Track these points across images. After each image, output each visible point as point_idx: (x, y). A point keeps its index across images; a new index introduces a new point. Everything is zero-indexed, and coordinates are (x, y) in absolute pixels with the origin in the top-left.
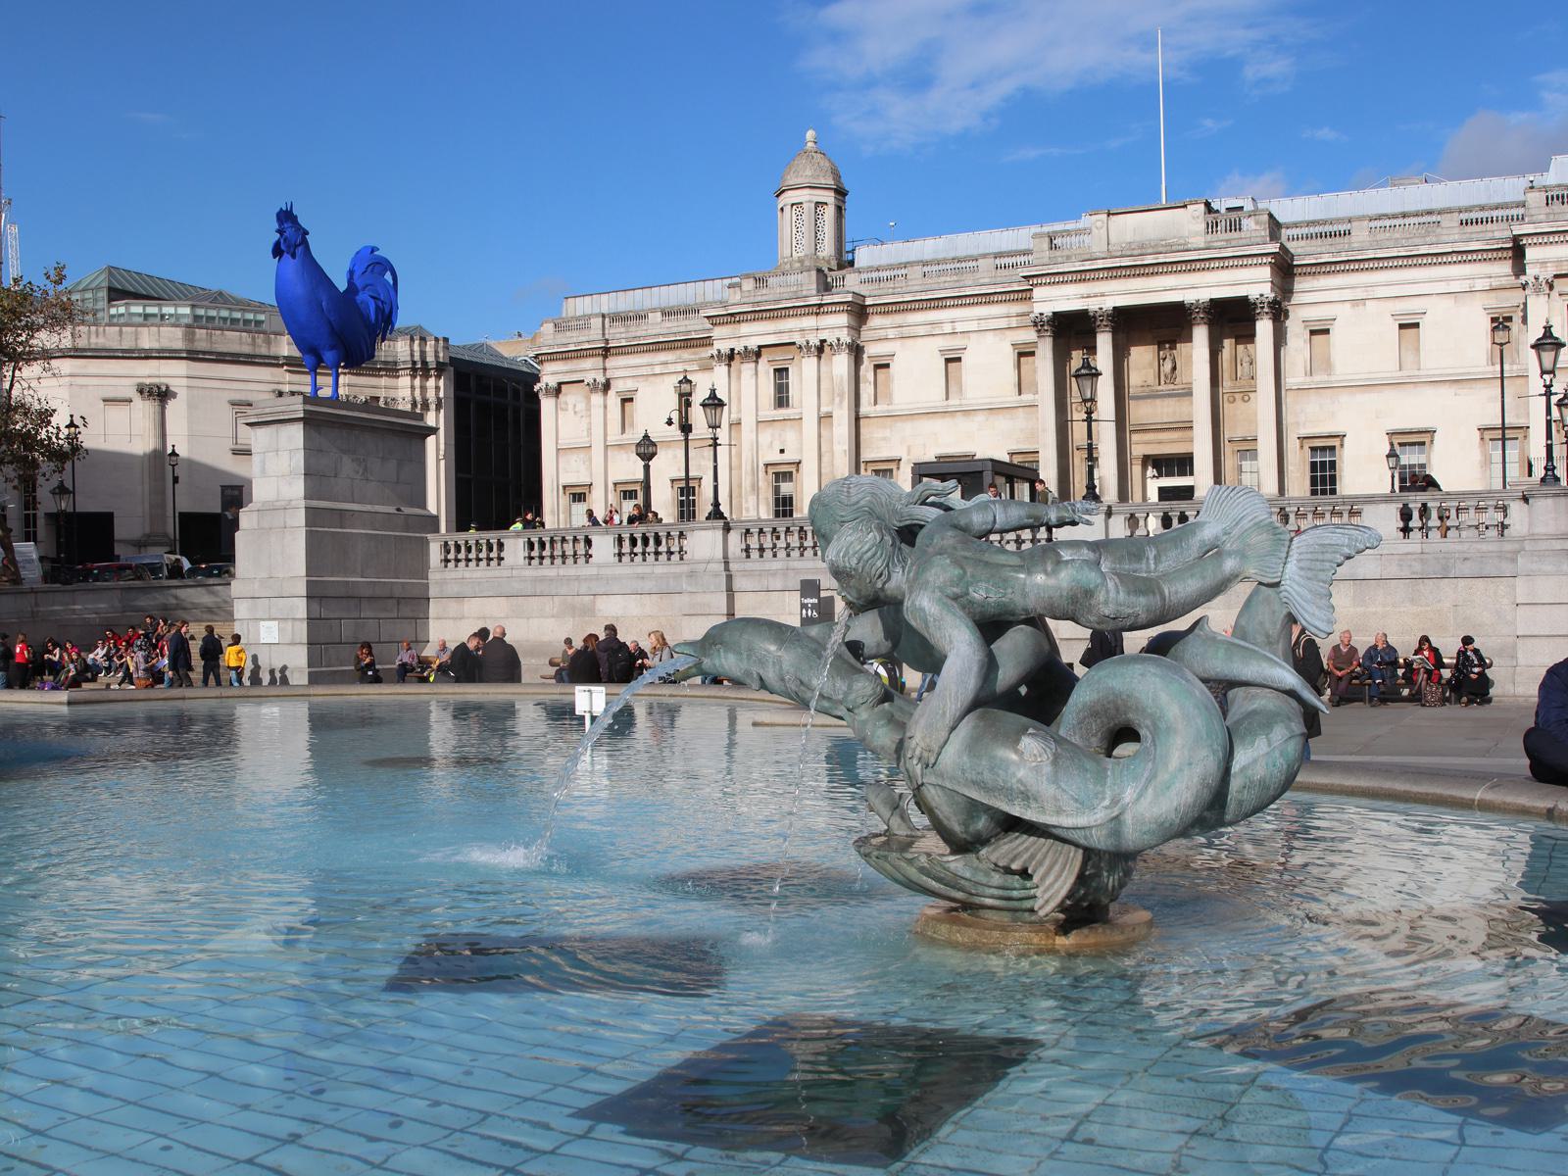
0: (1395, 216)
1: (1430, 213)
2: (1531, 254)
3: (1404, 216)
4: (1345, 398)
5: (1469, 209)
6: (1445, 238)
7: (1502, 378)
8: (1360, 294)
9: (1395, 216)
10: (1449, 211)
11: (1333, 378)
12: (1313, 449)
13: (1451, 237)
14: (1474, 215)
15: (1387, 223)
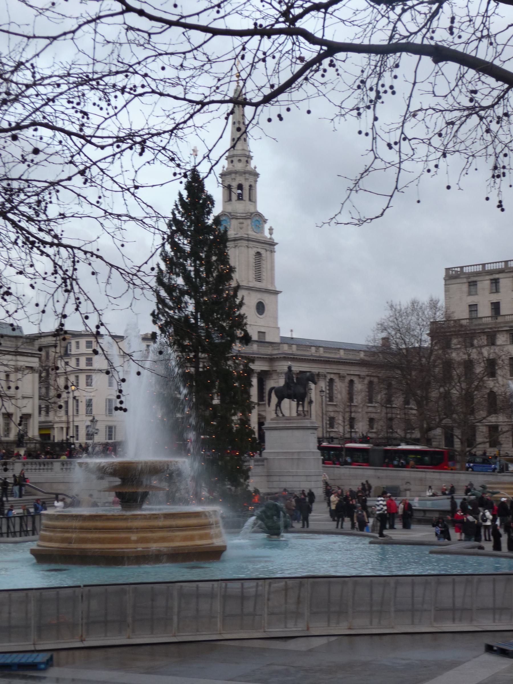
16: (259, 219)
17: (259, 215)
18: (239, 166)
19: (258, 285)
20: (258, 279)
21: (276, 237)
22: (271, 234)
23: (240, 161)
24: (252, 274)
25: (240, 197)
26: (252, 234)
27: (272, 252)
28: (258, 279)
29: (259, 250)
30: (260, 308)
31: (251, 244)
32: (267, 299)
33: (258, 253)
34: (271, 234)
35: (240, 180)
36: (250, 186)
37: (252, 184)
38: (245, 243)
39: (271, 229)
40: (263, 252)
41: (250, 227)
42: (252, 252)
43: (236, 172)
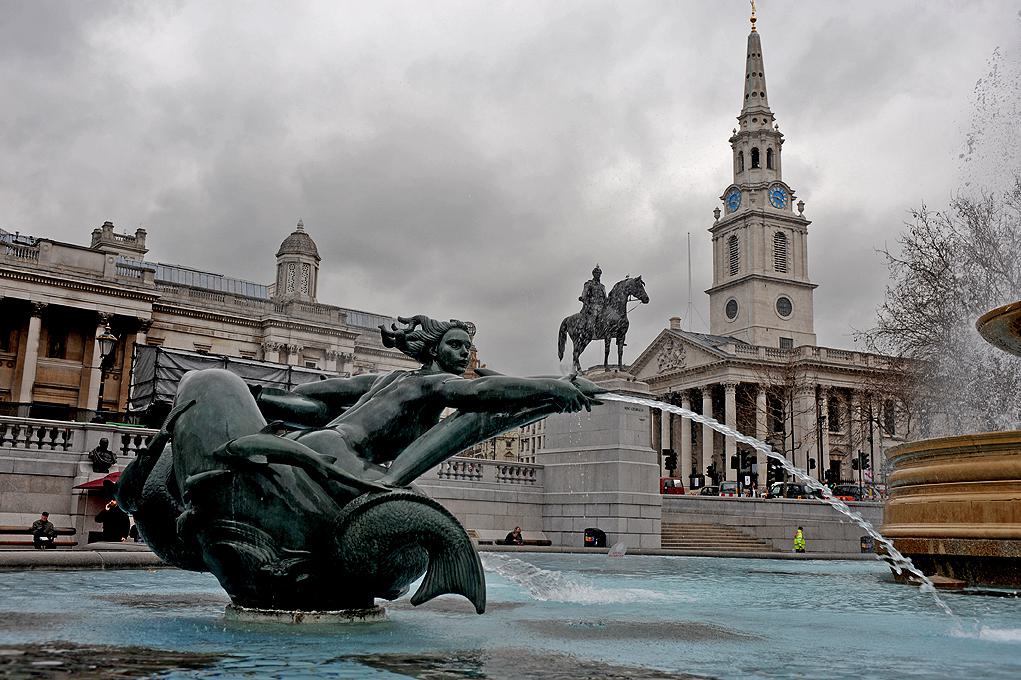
16: (784, 193)
17: (783, 186)
18: (753, 127)
19: (781, 275)
20: (782, 266)
21: (807, 215)
22: (801, 210)
23: (755, 120)
24: (770, 261)
25: (755, 165)
26: (769, 209)
27: (803, 233)
28: (782, 266)
29: (782, 230)
30: (784, 306)
31: (767, 221)
32: (794, 295)
33: (781, 235)
34: (801, 210)
35: (754, 143)
36: (770, 151)
37: (773, 147)
38: (757, 220)
39: (801, 204)
40: (787, 233)
41: (767, 199)
42: (771, 232)
43: (749, 134)
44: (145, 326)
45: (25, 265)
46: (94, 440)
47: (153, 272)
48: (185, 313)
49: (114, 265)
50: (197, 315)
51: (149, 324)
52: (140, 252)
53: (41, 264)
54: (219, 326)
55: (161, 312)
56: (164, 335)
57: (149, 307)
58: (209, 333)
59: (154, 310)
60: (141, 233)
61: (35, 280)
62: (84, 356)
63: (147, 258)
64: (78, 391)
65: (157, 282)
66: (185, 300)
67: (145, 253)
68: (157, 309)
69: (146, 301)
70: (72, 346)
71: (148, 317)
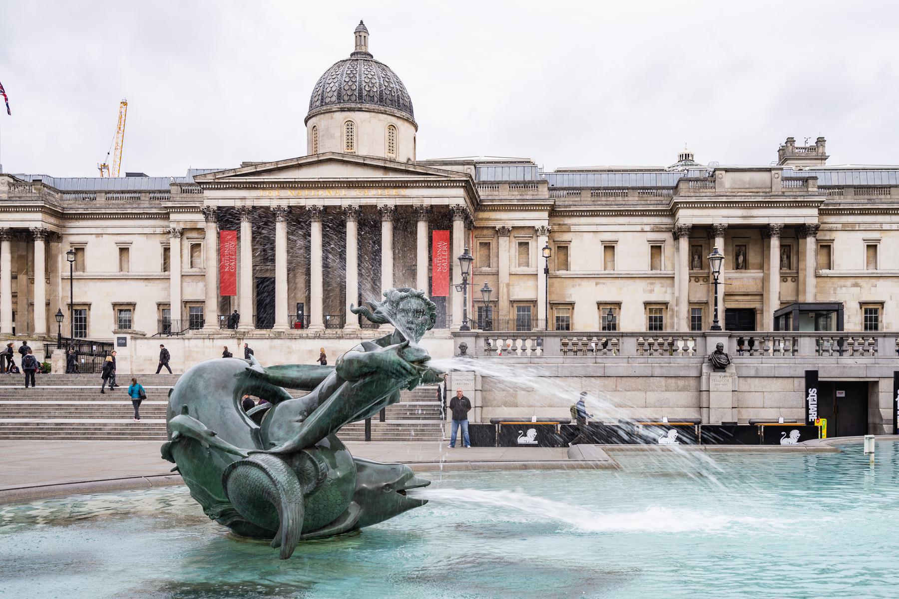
0: (118, 192)
1: (135, 192)
2: (173, 217)
3: (123, 192)
4: (91, 284)
5: (154, 192)
6: (142, 206)
7: (71, 279)
8: (99, 231)
9: (118, 192)
10: (145, 192)
11: (85, 274)
12: (121, 311)
13: (145, 205)
14: (158, 195)
15: (115, 195)
44: (815, 230)
45: (706, 195)
46: (712, 343)
47: (815, 178)
48: (852, 212)
49: (779, 179)
50: (863, 212)
51: (817, 228)
52: (822, 159)
53: (719, 190)
54: (887, 218)
55: (826, 214)
56: (834, 235)
57: (815, 212)
58: (877, 227)
59: (820, 214)
60: (821, 141)
61: (715, 205)
62: (763, 265)
63: (828, 164)
64: (762, 295)
65: (820, 187)
66: (847, 200)
67: (825, 159)
68: (822, 212)
69: (812, 207)
70: (753, 257)
71: (814, 221)
